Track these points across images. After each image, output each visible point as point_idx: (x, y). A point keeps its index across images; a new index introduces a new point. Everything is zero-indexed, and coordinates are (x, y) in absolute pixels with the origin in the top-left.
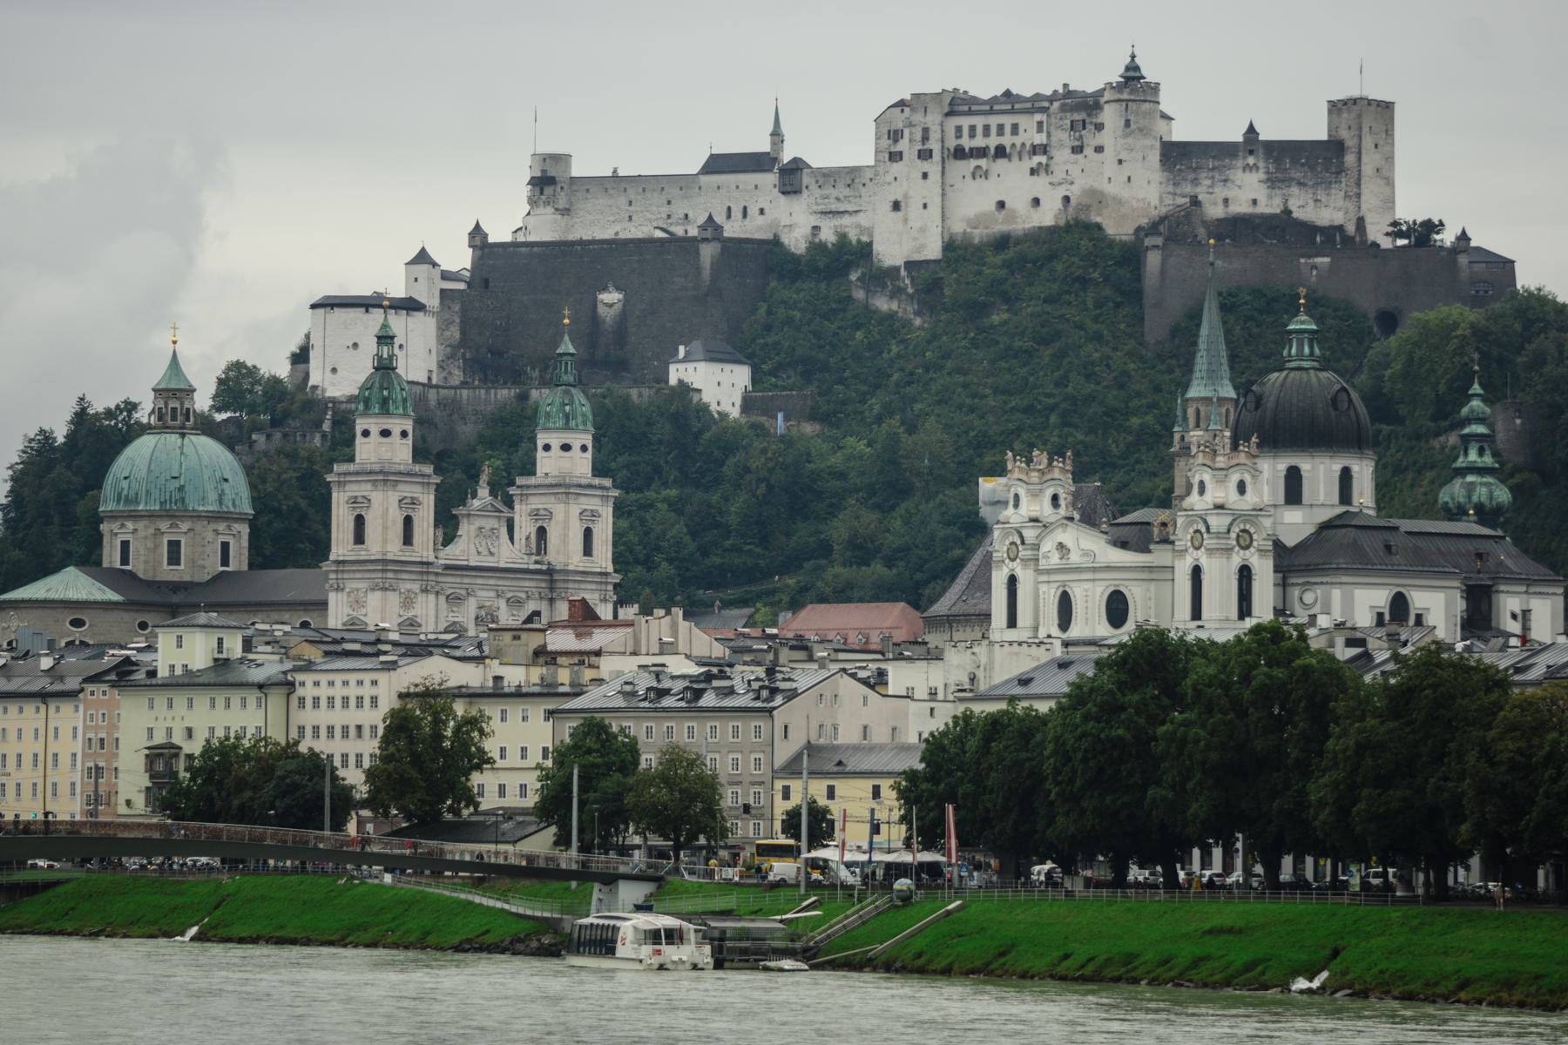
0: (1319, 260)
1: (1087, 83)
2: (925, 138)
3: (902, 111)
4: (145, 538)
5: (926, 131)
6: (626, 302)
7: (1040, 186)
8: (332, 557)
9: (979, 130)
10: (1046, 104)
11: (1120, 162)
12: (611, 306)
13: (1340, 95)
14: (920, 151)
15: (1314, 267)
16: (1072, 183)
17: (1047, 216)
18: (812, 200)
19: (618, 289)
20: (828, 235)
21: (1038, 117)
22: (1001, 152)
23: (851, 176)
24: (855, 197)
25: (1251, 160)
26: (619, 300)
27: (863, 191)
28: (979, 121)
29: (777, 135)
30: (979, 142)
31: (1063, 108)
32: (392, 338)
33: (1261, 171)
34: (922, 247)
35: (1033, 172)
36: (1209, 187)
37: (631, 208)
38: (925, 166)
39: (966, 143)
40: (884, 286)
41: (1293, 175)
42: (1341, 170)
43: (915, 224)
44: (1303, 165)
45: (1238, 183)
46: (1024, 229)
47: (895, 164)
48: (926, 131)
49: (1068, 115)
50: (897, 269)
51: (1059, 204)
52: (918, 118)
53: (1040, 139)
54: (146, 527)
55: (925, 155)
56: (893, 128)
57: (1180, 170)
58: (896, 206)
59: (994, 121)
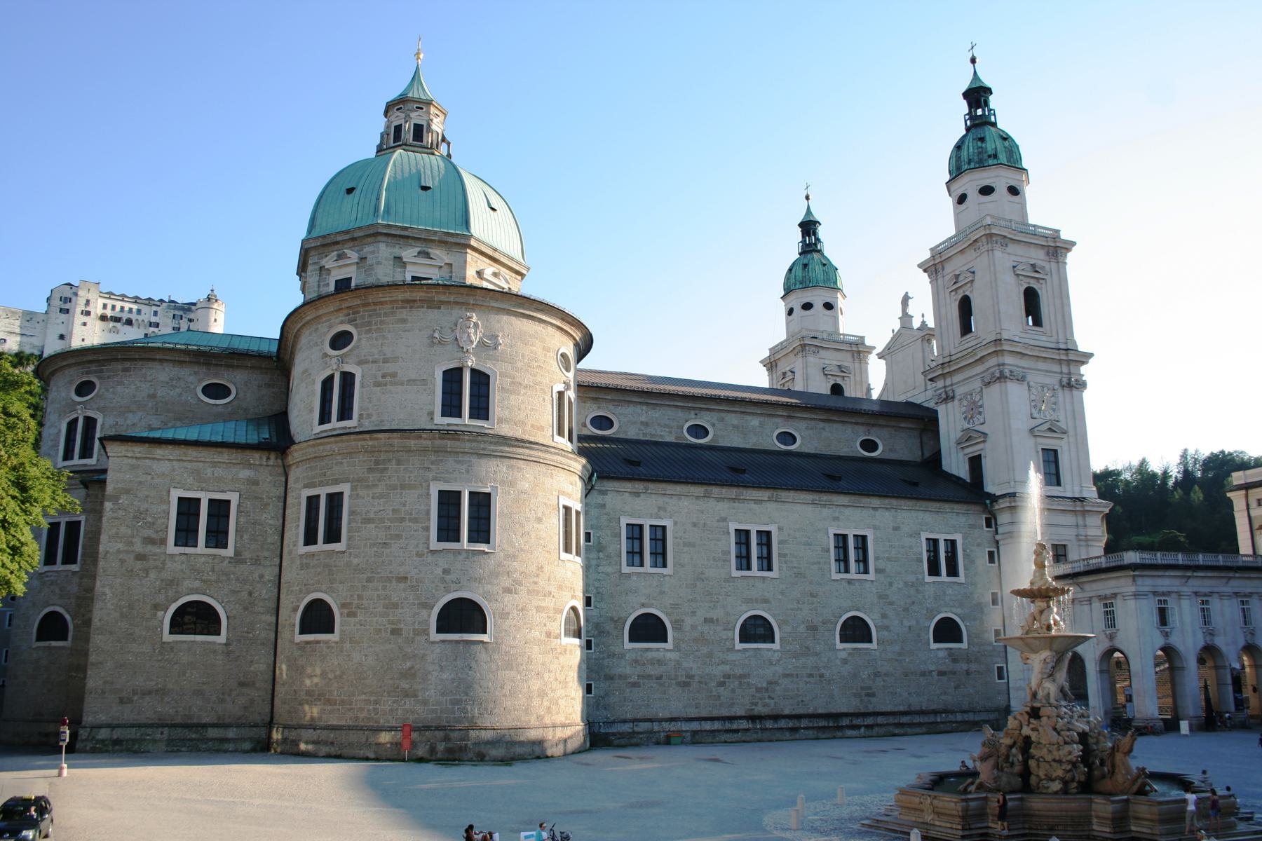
1: (182, 299)
5: (88, 302)
10: (158, 303)
21: (155, 308)
27: (37, 325)
28: (119, 305)
30: (117, 313)
31: (169, 307)
38: (85, 319)
48: (88, 302)
49: (172, 311)
53: (153, 319)
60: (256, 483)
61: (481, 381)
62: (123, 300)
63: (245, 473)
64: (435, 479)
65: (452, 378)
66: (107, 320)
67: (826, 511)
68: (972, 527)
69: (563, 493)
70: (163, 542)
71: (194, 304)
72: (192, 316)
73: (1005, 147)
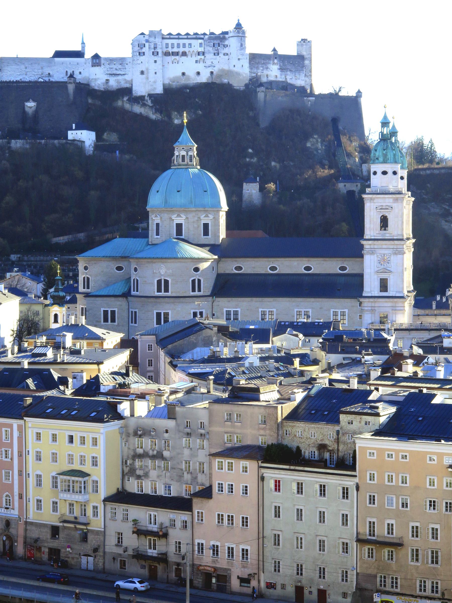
0: (311, 98)
2: (155, 48)
3: (144, 37)
4: (194, 222)
6: (37, 106)
7: (200, 67)
8: (366, 237)
9: (176, 45)
10: (202, 36)
11: (239, 59)
12: (31, 107)
13: (303, 38)
14: (153, 52)
15: (309, 101)
16: (214, 67)
17: (204, 78)
18: (106, 69)
19: (34, 101)
20: (114, 84)
21: (200, 41)
22: (184, 54)
23: (122, 61)
24: (123, 69)
25: (276, 61)
26: (34, 105)
27: (127, 66)
28: (175, 42)
29: (83, 43)
30: (175, 50)
31: (210, 38)
32: (389, 123)
33: (278, 65)
34: (155, 88)
35: (196, 62)
36: (262, 70)
37: (26, 70)
38: (156, 58)
39: (170, 50)
40: (138, 103)
41: (288, 67)
42: (303, 66)
43: (152, 79)
44: (291, 64)
45: (271, 69)
46: (195, 83)
47: (141, 57)
48: (155, 44)
50: (144, 97)
51: (209, 75)
52: (152, 39)
53: (201, 50)
54: (194, 217)
55: (155, 54)
56: (140, 43)
57: (253, 63)
58: (142, 73)
59: (181, 42)
60: (121, 305)
61: (166, 282)
62: (179, 38)
63: (119, 303)
64: (155, 309)
65: (159, 282)
66: (170, 55)
67: (294, 304)
68: (353, 306)
69: (193, 309)
70: (100, 322)
71: (227, 33)
72: (226, 43)
73: (383, 154)
